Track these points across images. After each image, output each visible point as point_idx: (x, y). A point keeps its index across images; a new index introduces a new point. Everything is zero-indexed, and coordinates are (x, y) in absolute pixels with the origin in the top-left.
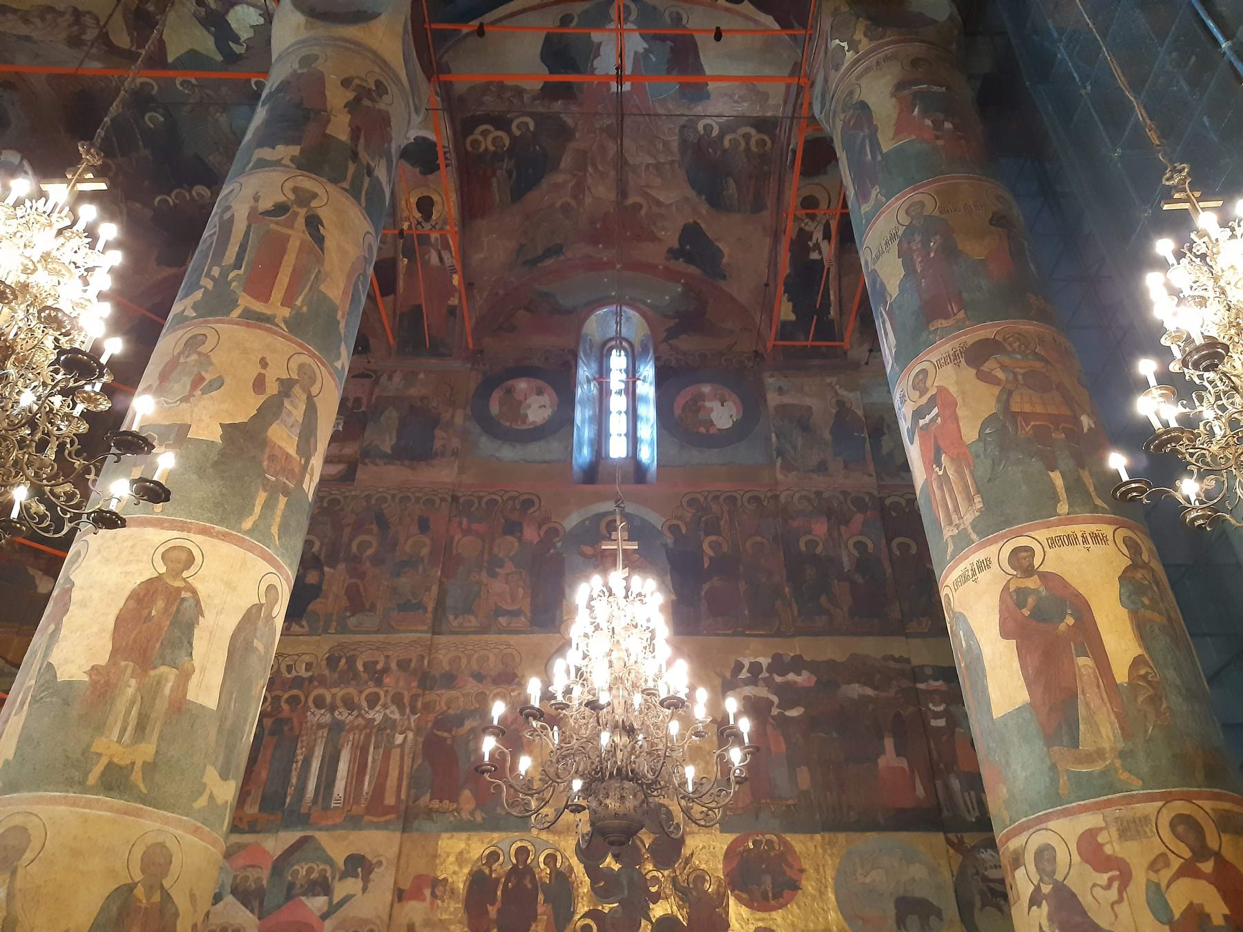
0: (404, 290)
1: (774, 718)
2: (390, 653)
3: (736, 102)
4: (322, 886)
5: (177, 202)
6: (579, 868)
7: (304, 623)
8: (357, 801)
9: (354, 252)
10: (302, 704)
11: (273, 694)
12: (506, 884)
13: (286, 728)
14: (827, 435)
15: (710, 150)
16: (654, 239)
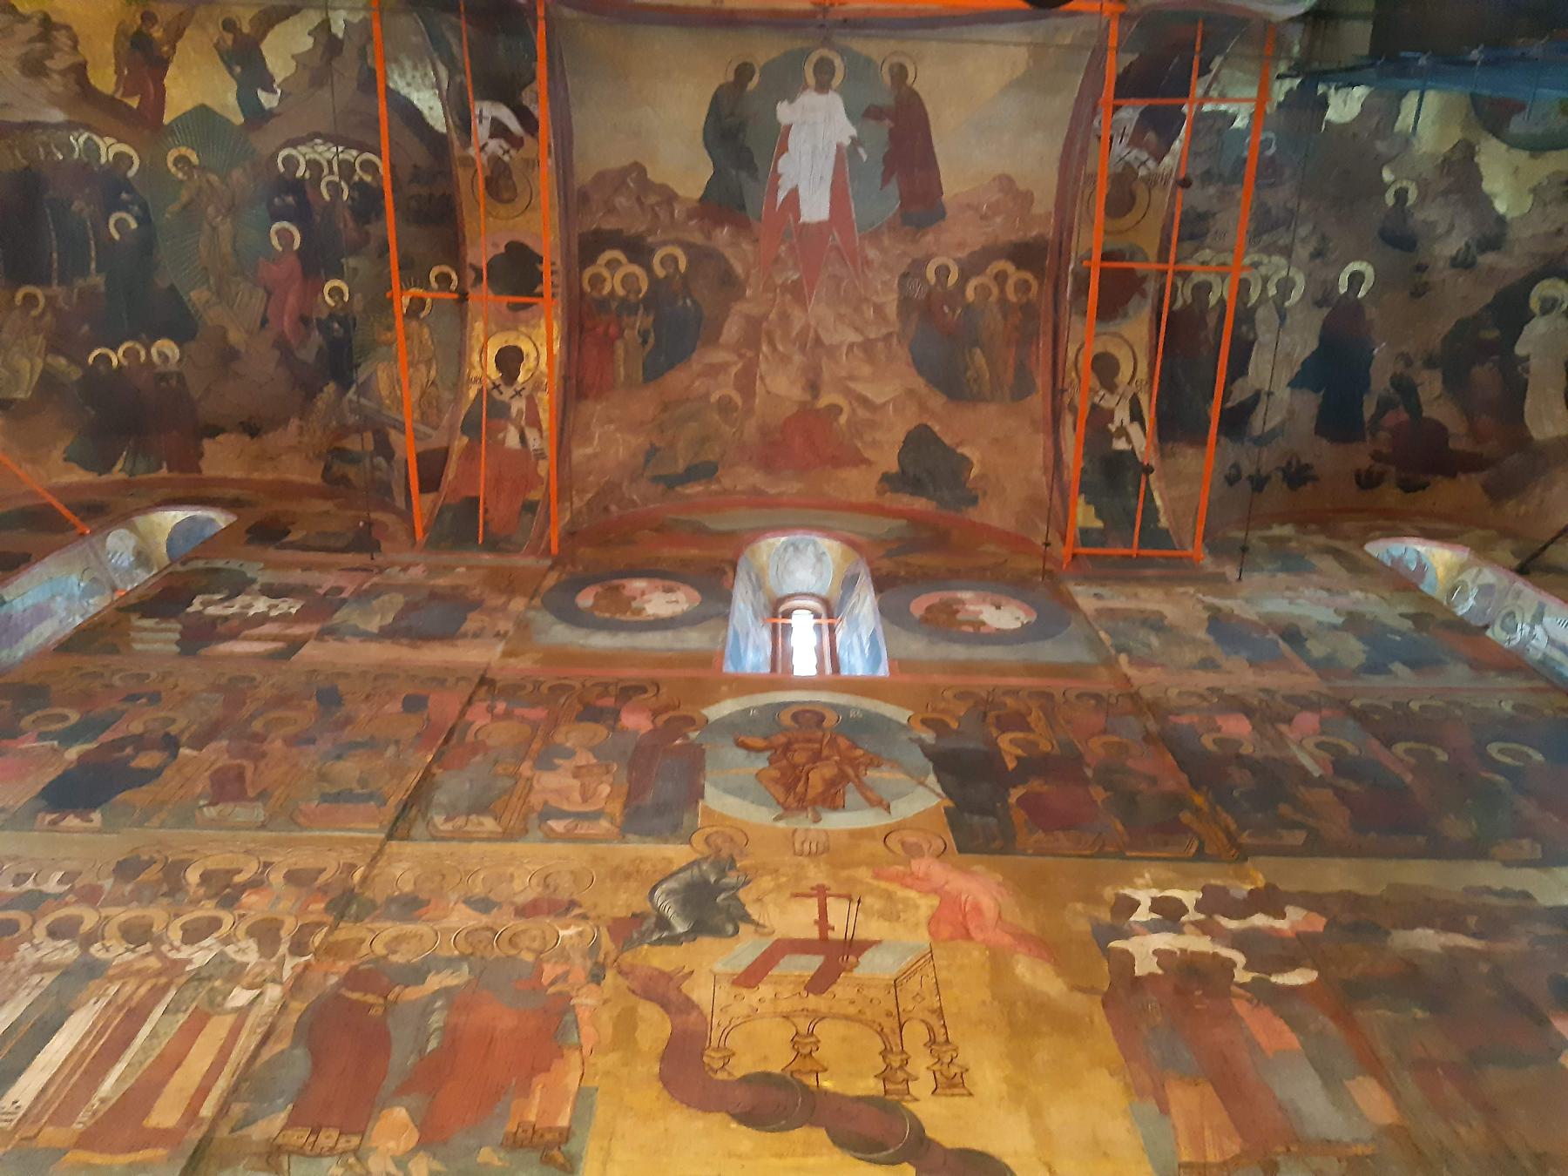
0: (456, 477)
1: (1242, 986)
2: (275, 859)
3: (984, 217)
5: (125, 362)
8: (63, 1115)
14: (1202, 634)
15: (946, 309)
16: (860, 461)
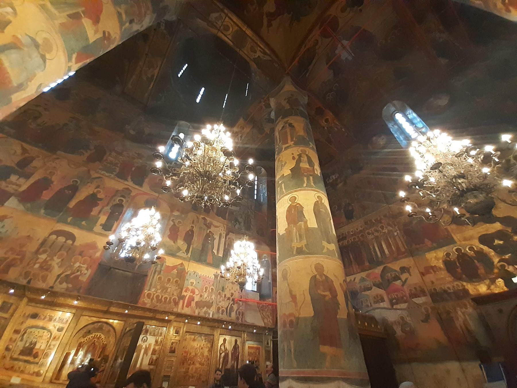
4: (397, 278)
6: (485, 248)
9: (302, 125)
11: (357, 236)
12: (458, 260)
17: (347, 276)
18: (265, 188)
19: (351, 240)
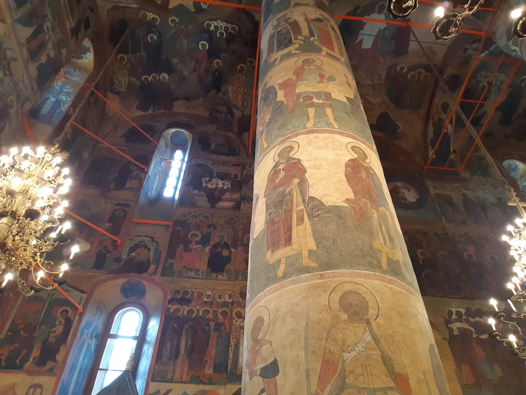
1: (474, 338)
5: (152, 80)
7: (225, 274)
10: (229, 316)
11: (214, 309)
13: (222, 328)
15: (401, 79)
17: (153, 380)
18: (68, 94)
19: (198, 311)
